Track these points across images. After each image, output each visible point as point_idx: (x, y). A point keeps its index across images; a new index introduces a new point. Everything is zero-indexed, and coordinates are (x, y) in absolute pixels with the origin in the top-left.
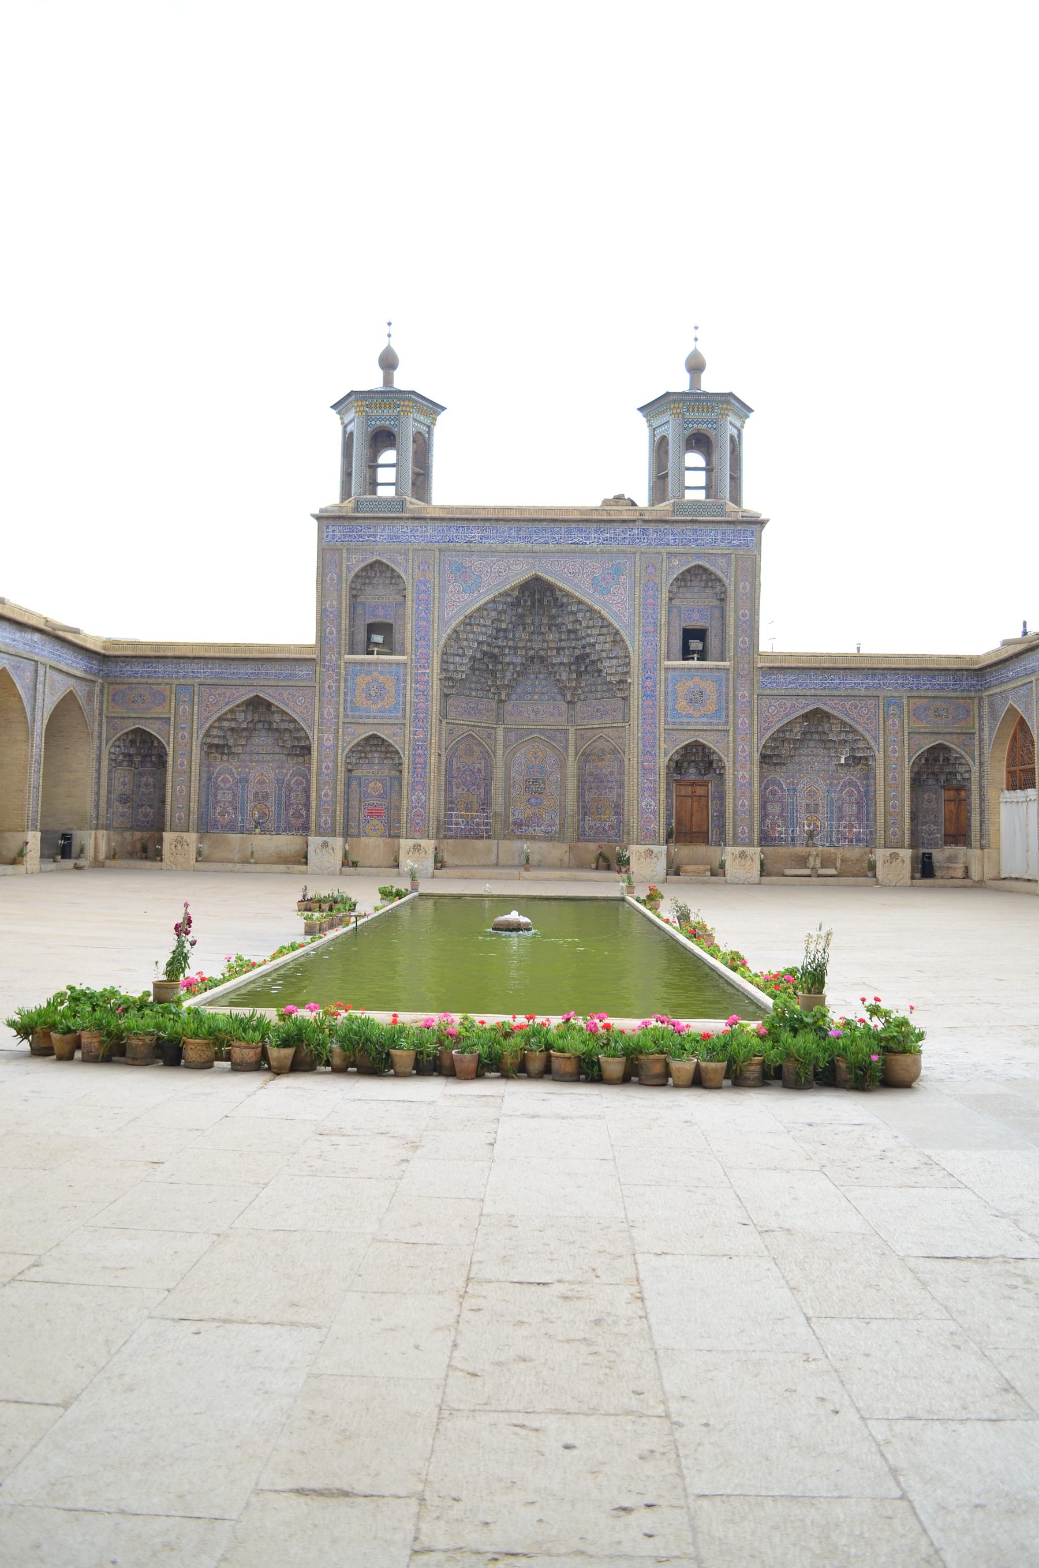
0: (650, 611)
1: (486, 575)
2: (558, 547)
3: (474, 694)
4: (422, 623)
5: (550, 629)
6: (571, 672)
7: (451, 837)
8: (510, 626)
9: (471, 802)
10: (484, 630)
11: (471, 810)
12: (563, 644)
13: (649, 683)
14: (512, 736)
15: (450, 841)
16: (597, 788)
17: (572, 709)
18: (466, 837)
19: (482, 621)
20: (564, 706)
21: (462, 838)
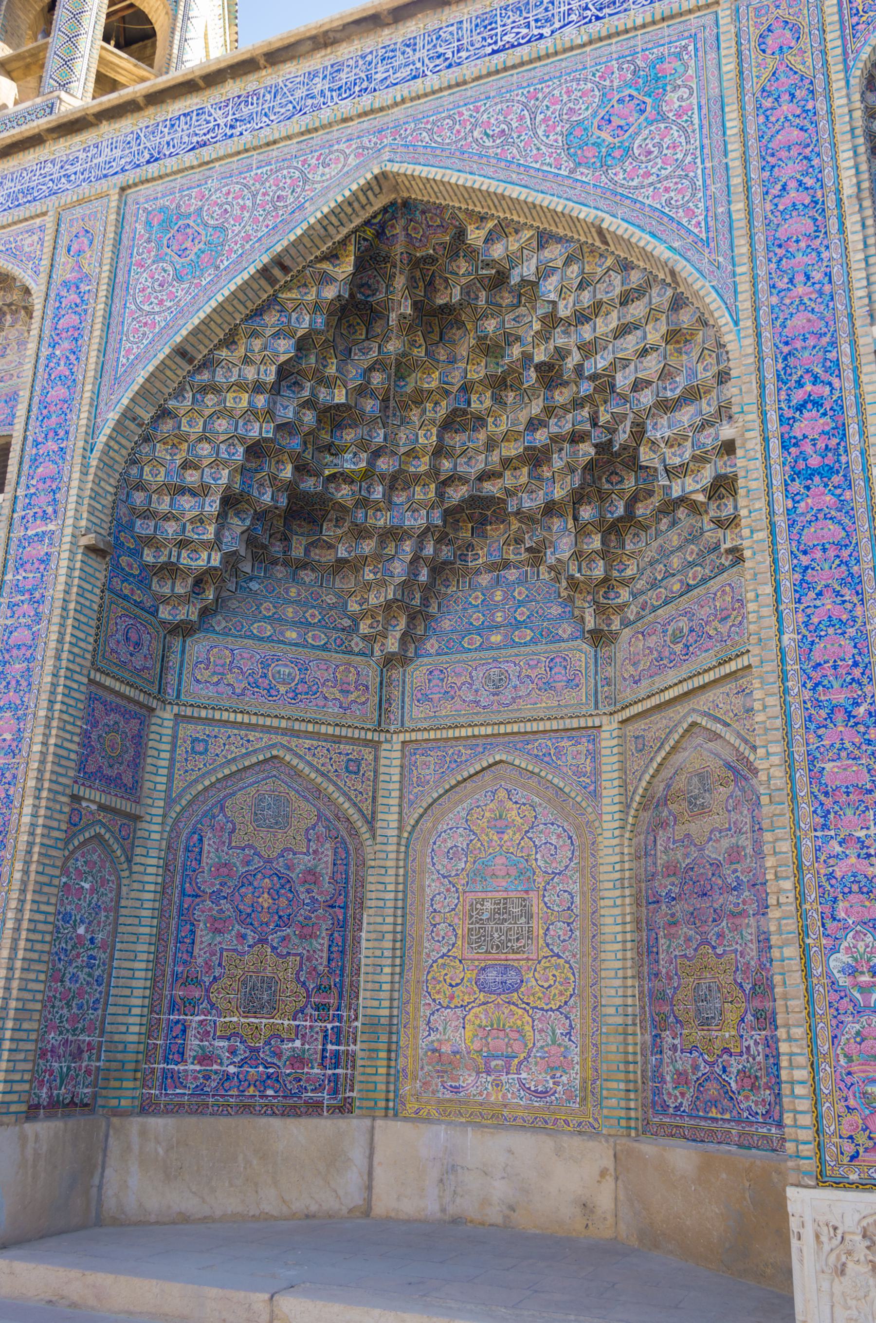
0: (789, 170)
1: (239, 219)
2: (451, 75)
3: (291, 635)
4: (59, 392)
5: (498, 400)
6: (581, 531)
7: (173, 1109)
8: (370, 405)
9: (270, 983)
10: (261, 400)
11: (273, 1008)
12: (541, 437)
13: (809, 424)
14: (428, 766)
15: (159, 1124)
16: (693, 917)
17: (611, 660)
18: (246, 1109)
19: (250, 373)
20: (581, 654)
21: (224, 1111)
